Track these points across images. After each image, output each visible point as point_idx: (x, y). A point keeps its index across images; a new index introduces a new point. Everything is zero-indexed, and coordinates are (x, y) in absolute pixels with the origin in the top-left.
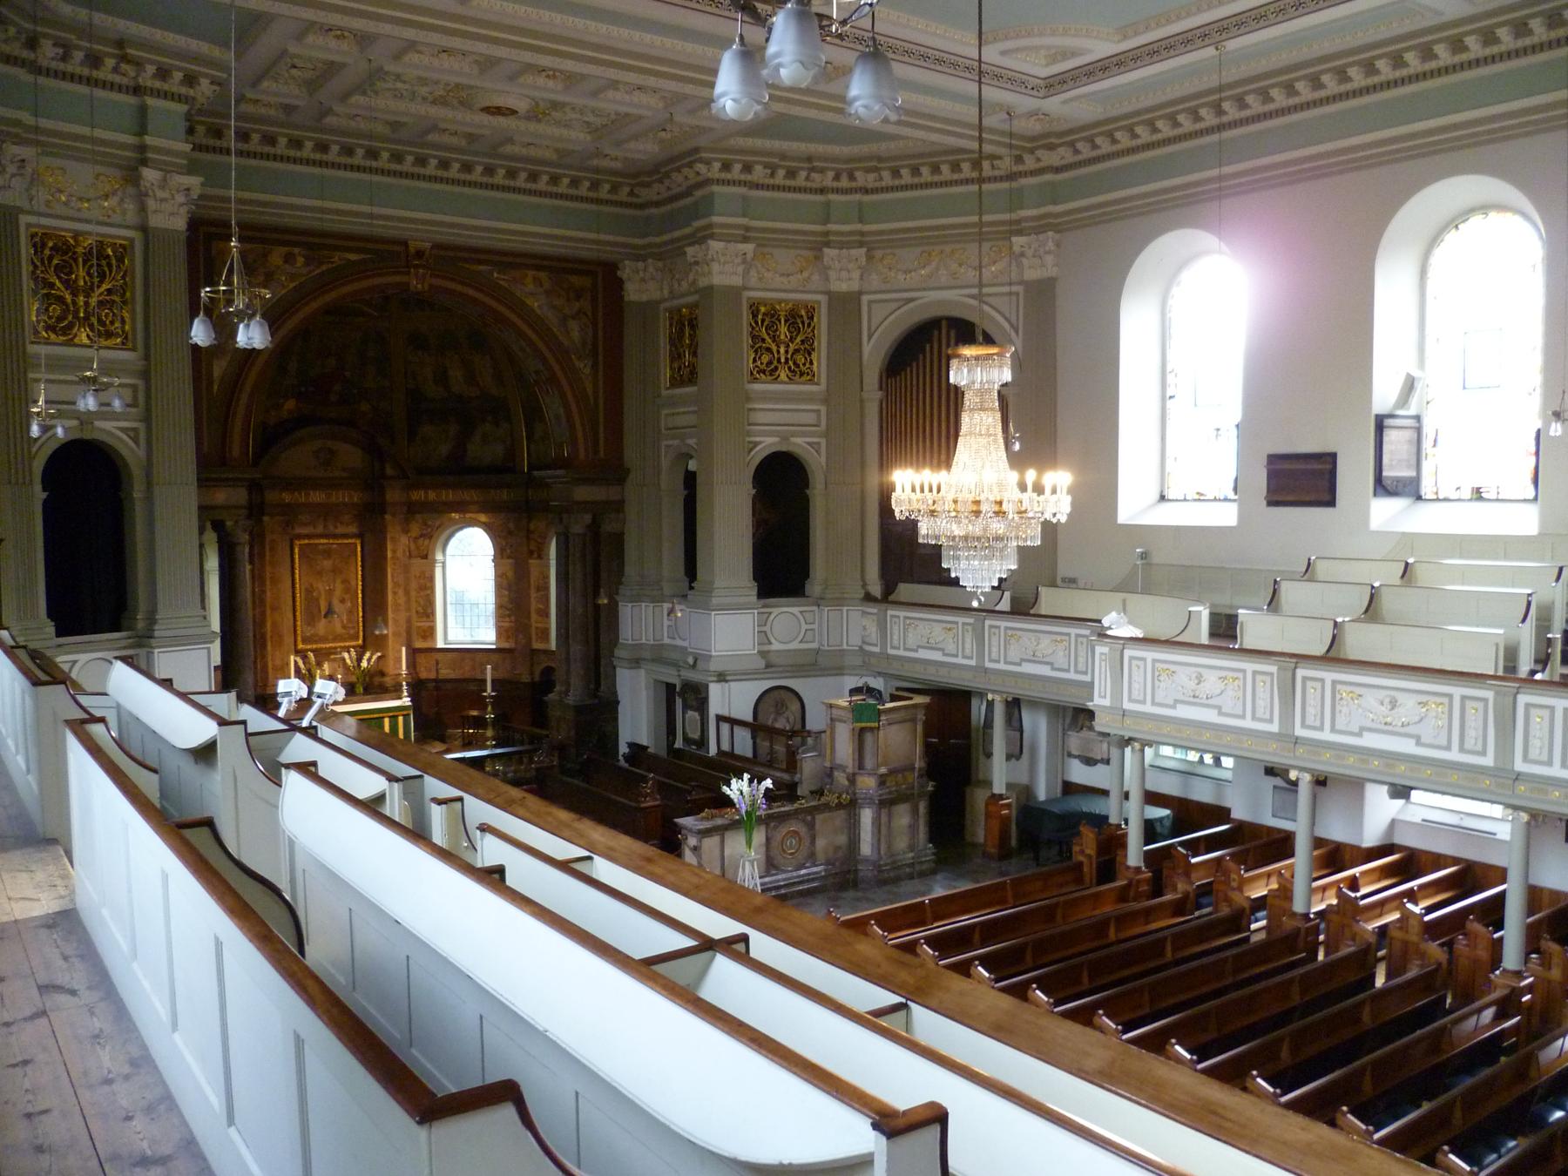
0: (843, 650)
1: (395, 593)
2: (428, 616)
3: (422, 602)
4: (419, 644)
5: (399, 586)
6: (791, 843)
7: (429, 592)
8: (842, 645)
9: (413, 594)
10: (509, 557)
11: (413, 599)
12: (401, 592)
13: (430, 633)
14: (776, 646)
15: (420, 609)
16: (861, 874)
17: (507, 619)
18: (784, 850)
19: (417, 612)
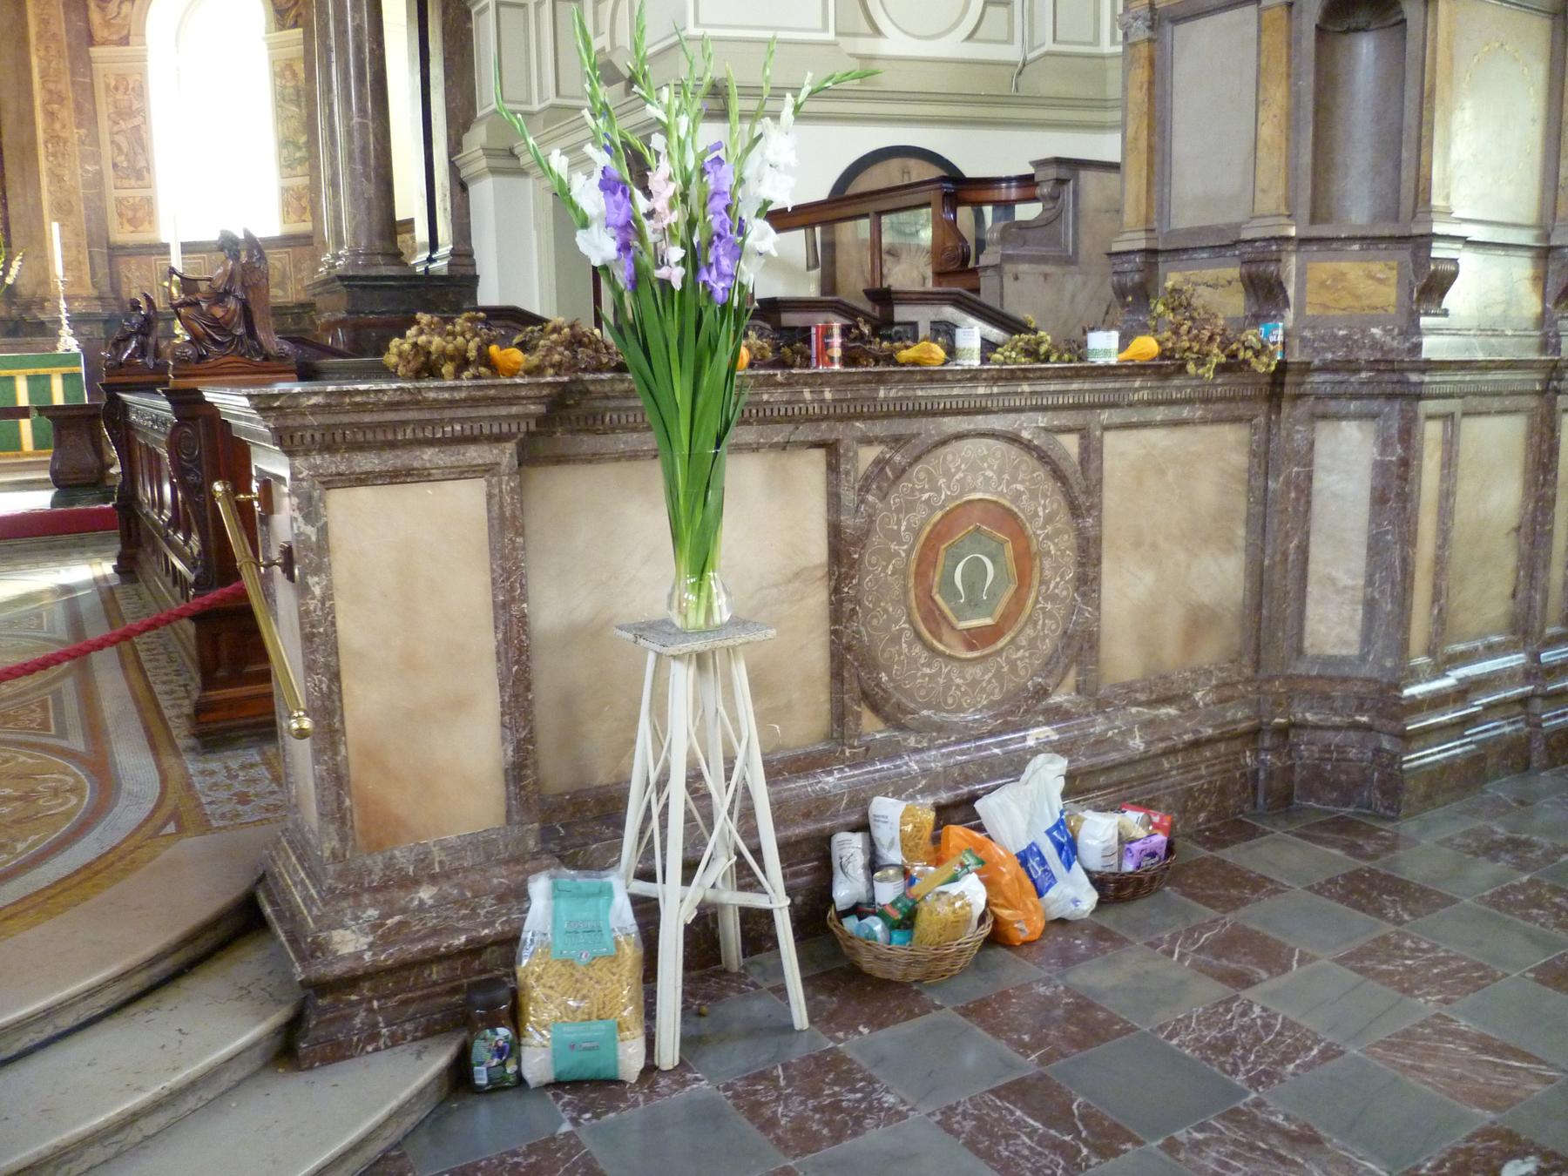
0: (1102, 57)
1: (51, 116)
2: (139, 177)
3: (125, 147)
4: (122, 235)
5: (61, 100)
6: (976, 569)
7: (137, 121)
8: (1096, 41)
9: (104, 124)
10: (295, 25)
11: (105, 137)
12: (66, 113)
13: (142, 212)
14: (893, 44)
15: (121, 159)
16: (1307, 750)
17: (299, 170)
18: (934, 617)
19: (115, 165)
